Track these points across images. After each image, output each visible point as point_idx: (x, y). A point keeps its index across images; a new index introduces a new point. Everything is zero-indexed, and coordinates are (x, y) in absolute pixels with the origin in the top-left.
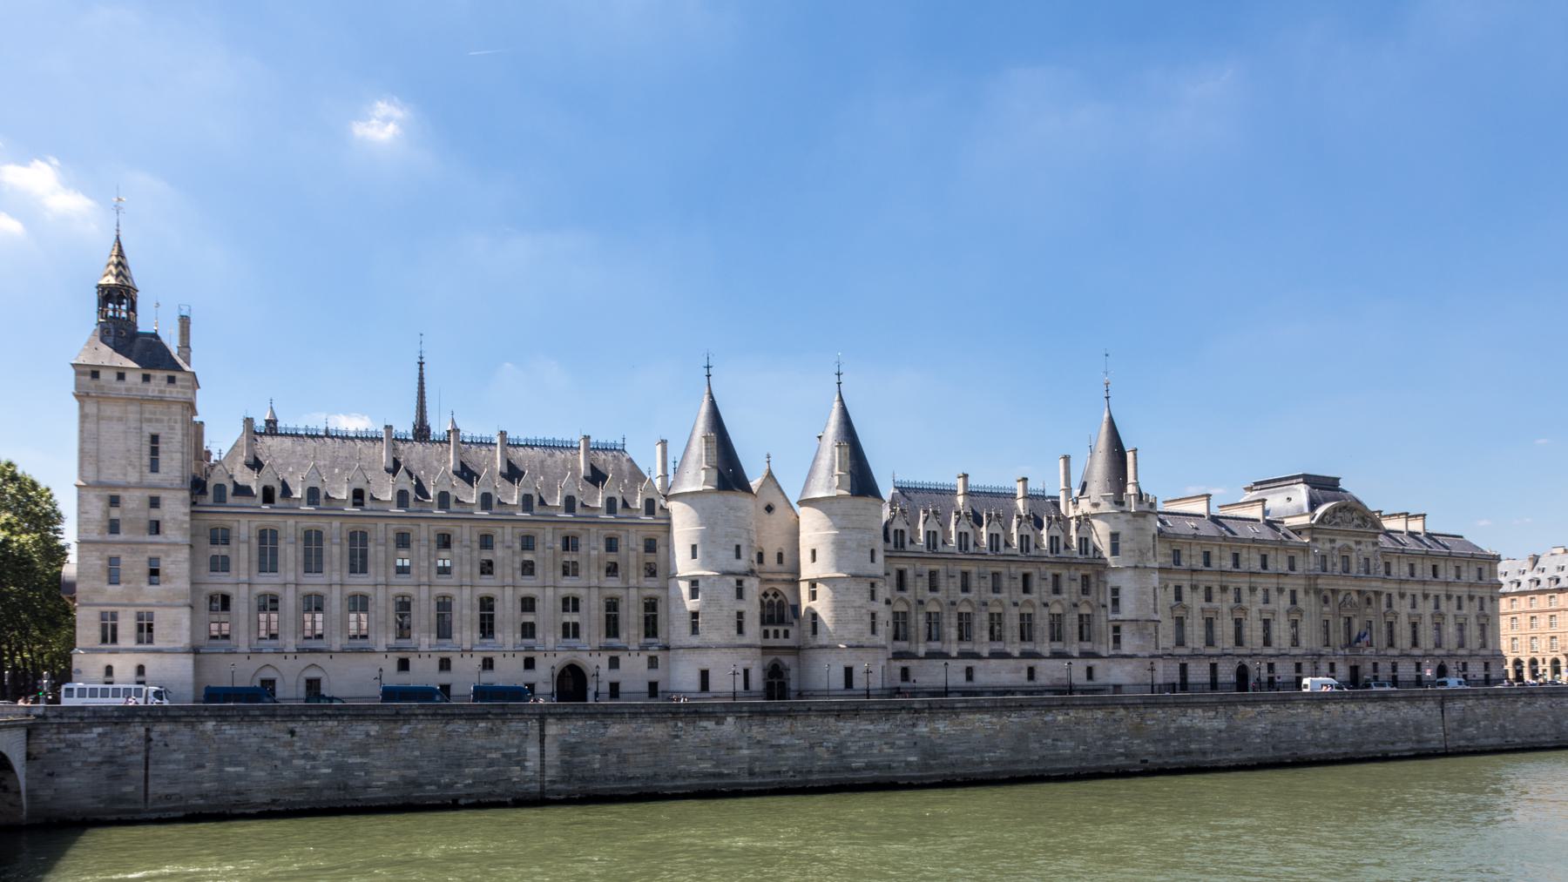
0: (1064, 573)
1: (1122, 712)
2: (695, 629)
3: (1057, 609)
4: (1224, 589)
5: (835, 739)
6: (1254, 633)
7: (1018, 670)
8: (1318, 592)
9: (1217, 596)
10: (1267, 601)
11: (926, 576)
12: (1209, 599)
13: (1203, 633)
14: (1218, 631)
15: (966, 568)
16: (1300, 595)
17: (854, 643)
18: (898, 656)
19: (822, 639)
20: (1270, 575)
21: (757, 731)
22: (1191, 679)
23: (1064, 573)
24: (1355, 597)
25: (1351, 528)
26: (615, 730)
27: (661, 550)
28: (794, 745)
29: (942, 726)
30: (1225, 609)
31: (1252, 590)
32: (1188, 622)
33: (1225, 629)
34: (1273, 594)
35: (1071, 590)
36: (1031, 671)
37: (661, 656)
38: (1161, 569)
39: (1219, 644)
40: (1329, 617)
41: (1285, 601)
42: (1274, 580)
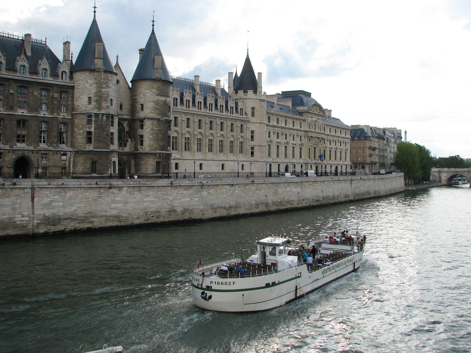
0: (235, 123)
1: (271, 185)
2: (89, 140)
3: (232, 139)
4: (282, 134)
5: (171, 198)
6: (290, 152)
7: (218, 166)
8: (308, 137)
10: (294, 140)
11: (186, 121)
12: (278, 138)
13: (276, 152)
15: (200, 118)
16: (303, 138)
20: (295, 130)
21: (138, 195)
22: (273, 171)
26: (70, 194)
28: (152, 201)
29: (212, 191)
30: (283, 143)
32: (272, 147)
33: (282, 149)
34: (295, 136)
36: (223, 165)
38: (267, 125)
39: (280, 156)
40: (310, 147)
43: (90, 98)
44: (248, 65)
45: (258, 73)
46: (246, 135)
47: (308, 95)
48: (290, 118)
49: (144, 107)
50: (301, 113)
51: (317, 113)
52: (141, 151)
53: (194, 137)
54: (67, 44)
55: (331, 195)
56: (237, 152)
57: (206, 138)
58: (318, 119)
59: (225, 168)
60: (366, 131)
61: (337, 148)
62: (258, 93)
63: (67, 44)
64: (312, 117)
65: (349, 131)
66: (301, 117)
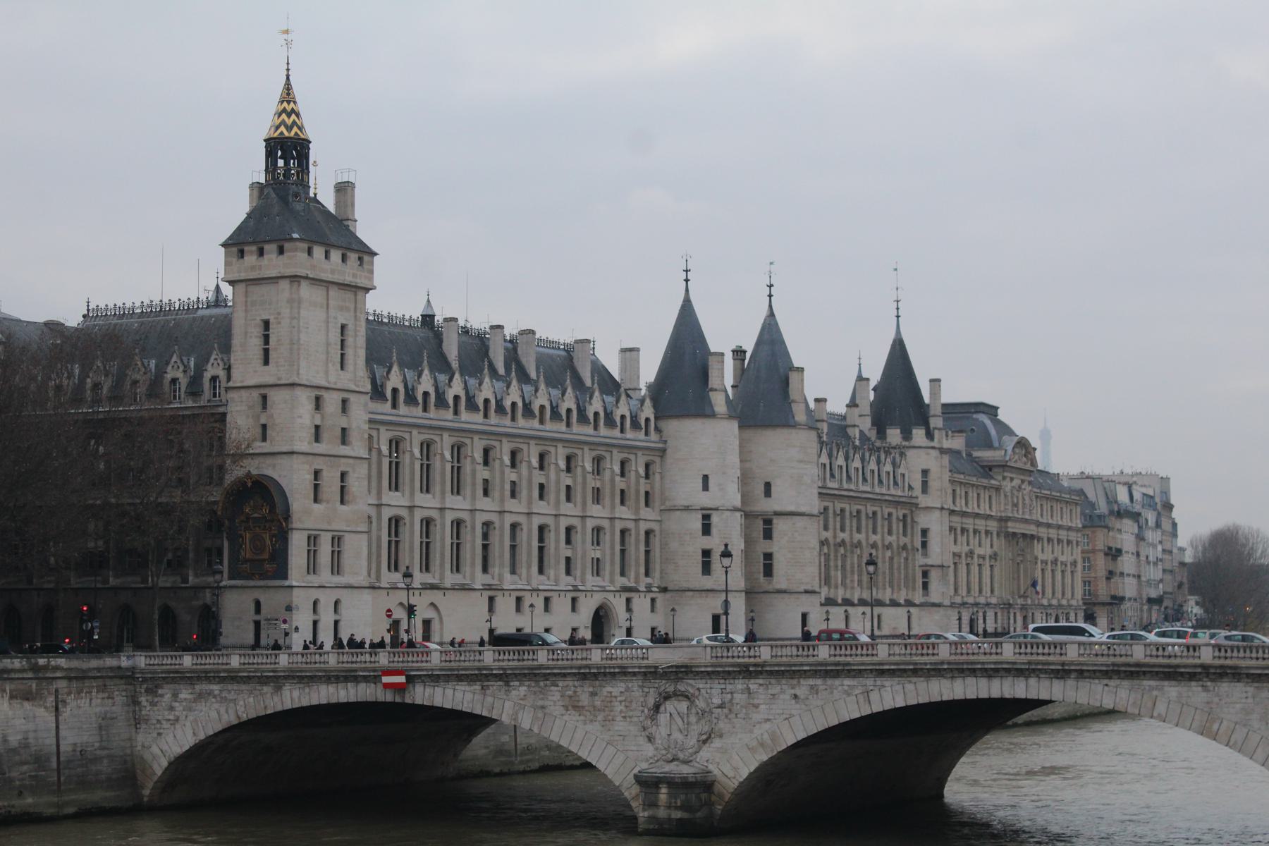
17: (809, 588)
19: (780, 581)
23: (894, 511)
27: (657, 477)
35: (897, 527)
37: (660, 598)
42: (983, 522)
43: (706, 478)
44: (899, 357)
45: (932, 381)
46: (912, 541)
47: (992, 410)
48: (973, 485)
49: (773, 489)
50: (988, 469)
51: (1020, 465)
52: (770, 588)
53: (836, 551)
54: (630, 353)
56: (899, 586)
57: (852, 552)
58: (1023, 481)
59: (883, 624)
60: (1091, 496)
61: (1055, 562)
62: (936, 433)
63: (630, 353)
64: (1012, 479)
65: (1079, 509)
66: (993, 482)
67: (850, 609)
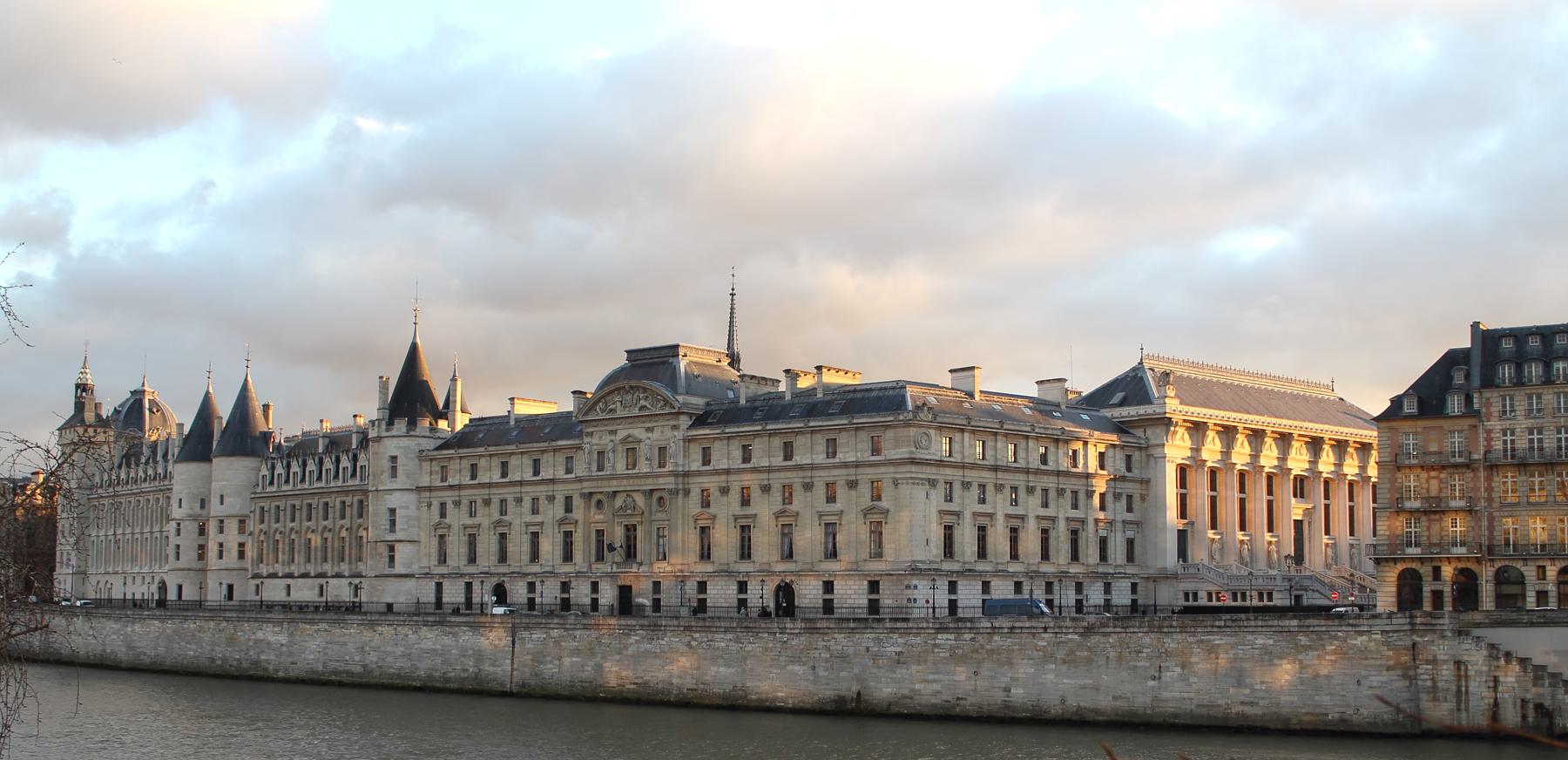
6: (519, 547)
7: (312, 588)
9: (481, 510)
14: (480, 548)
16: (577, 502)
18: (255, 576)
23: (348, 500)
24: (640, 500)
25: (636, 412)
29: (137, 627)
30: (486, 523)
31: (519, 501)
41: (559, 510)
55: (403, 663)
64: (614, 432)
67: (289, 581)
